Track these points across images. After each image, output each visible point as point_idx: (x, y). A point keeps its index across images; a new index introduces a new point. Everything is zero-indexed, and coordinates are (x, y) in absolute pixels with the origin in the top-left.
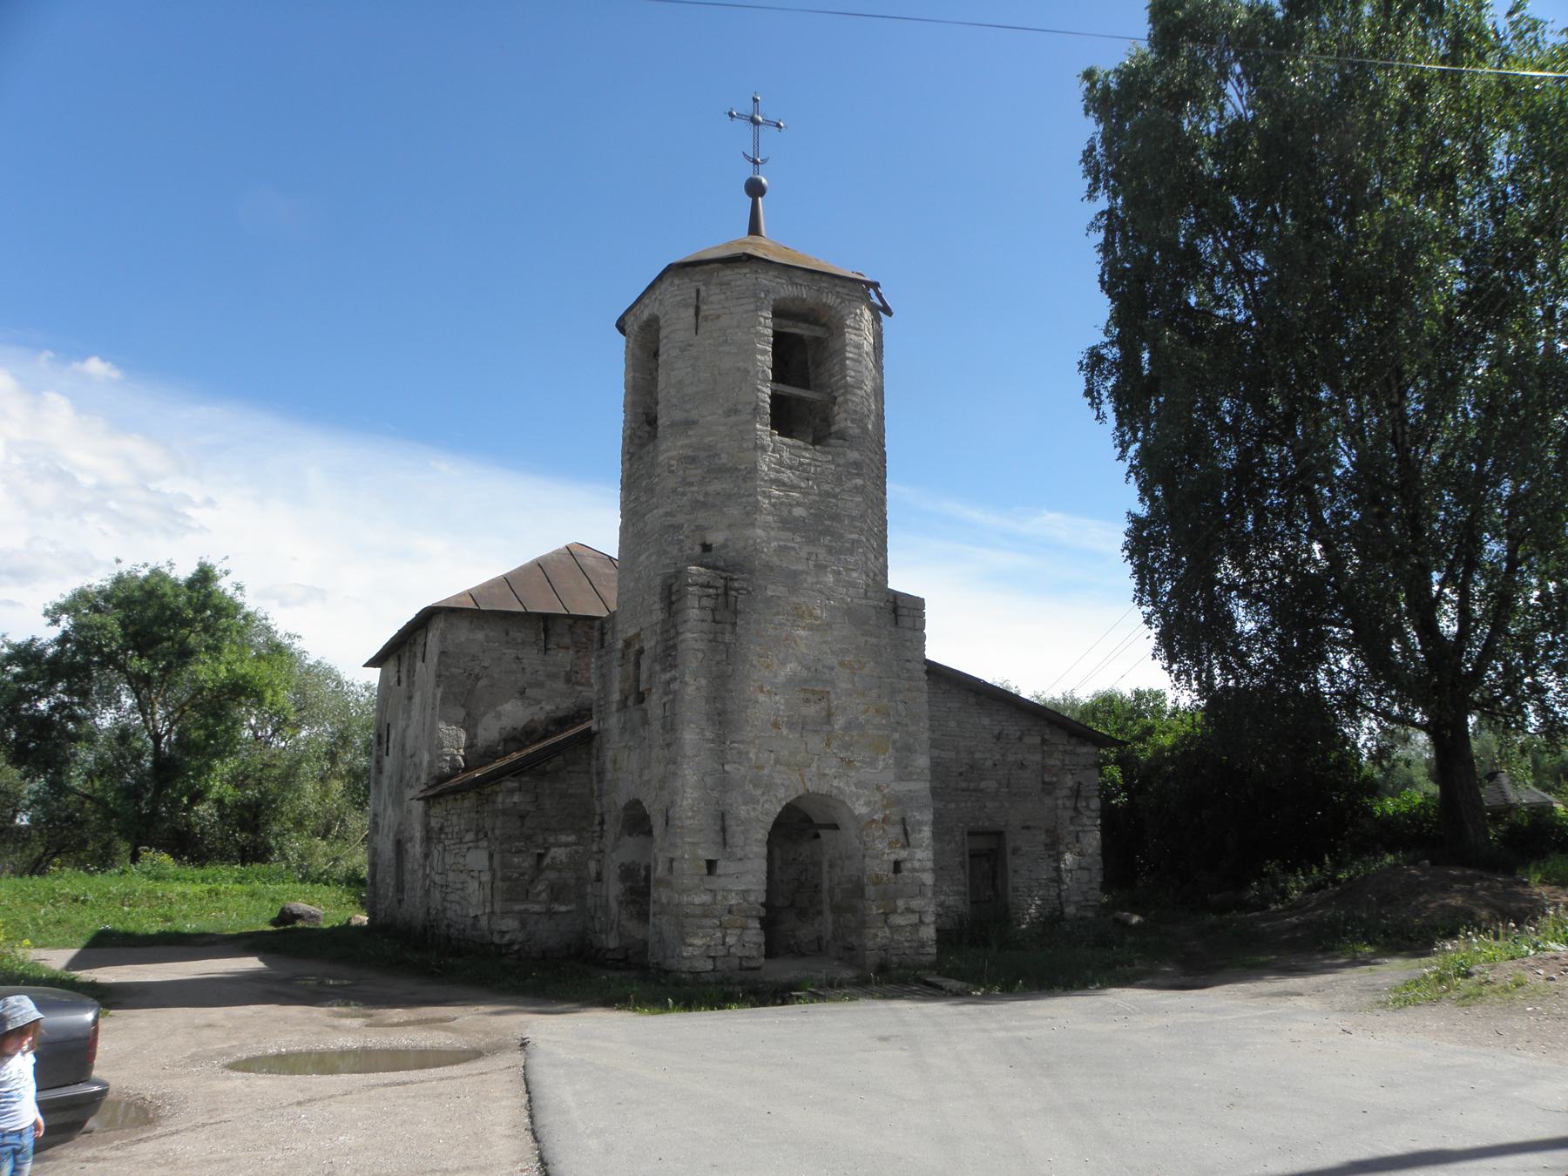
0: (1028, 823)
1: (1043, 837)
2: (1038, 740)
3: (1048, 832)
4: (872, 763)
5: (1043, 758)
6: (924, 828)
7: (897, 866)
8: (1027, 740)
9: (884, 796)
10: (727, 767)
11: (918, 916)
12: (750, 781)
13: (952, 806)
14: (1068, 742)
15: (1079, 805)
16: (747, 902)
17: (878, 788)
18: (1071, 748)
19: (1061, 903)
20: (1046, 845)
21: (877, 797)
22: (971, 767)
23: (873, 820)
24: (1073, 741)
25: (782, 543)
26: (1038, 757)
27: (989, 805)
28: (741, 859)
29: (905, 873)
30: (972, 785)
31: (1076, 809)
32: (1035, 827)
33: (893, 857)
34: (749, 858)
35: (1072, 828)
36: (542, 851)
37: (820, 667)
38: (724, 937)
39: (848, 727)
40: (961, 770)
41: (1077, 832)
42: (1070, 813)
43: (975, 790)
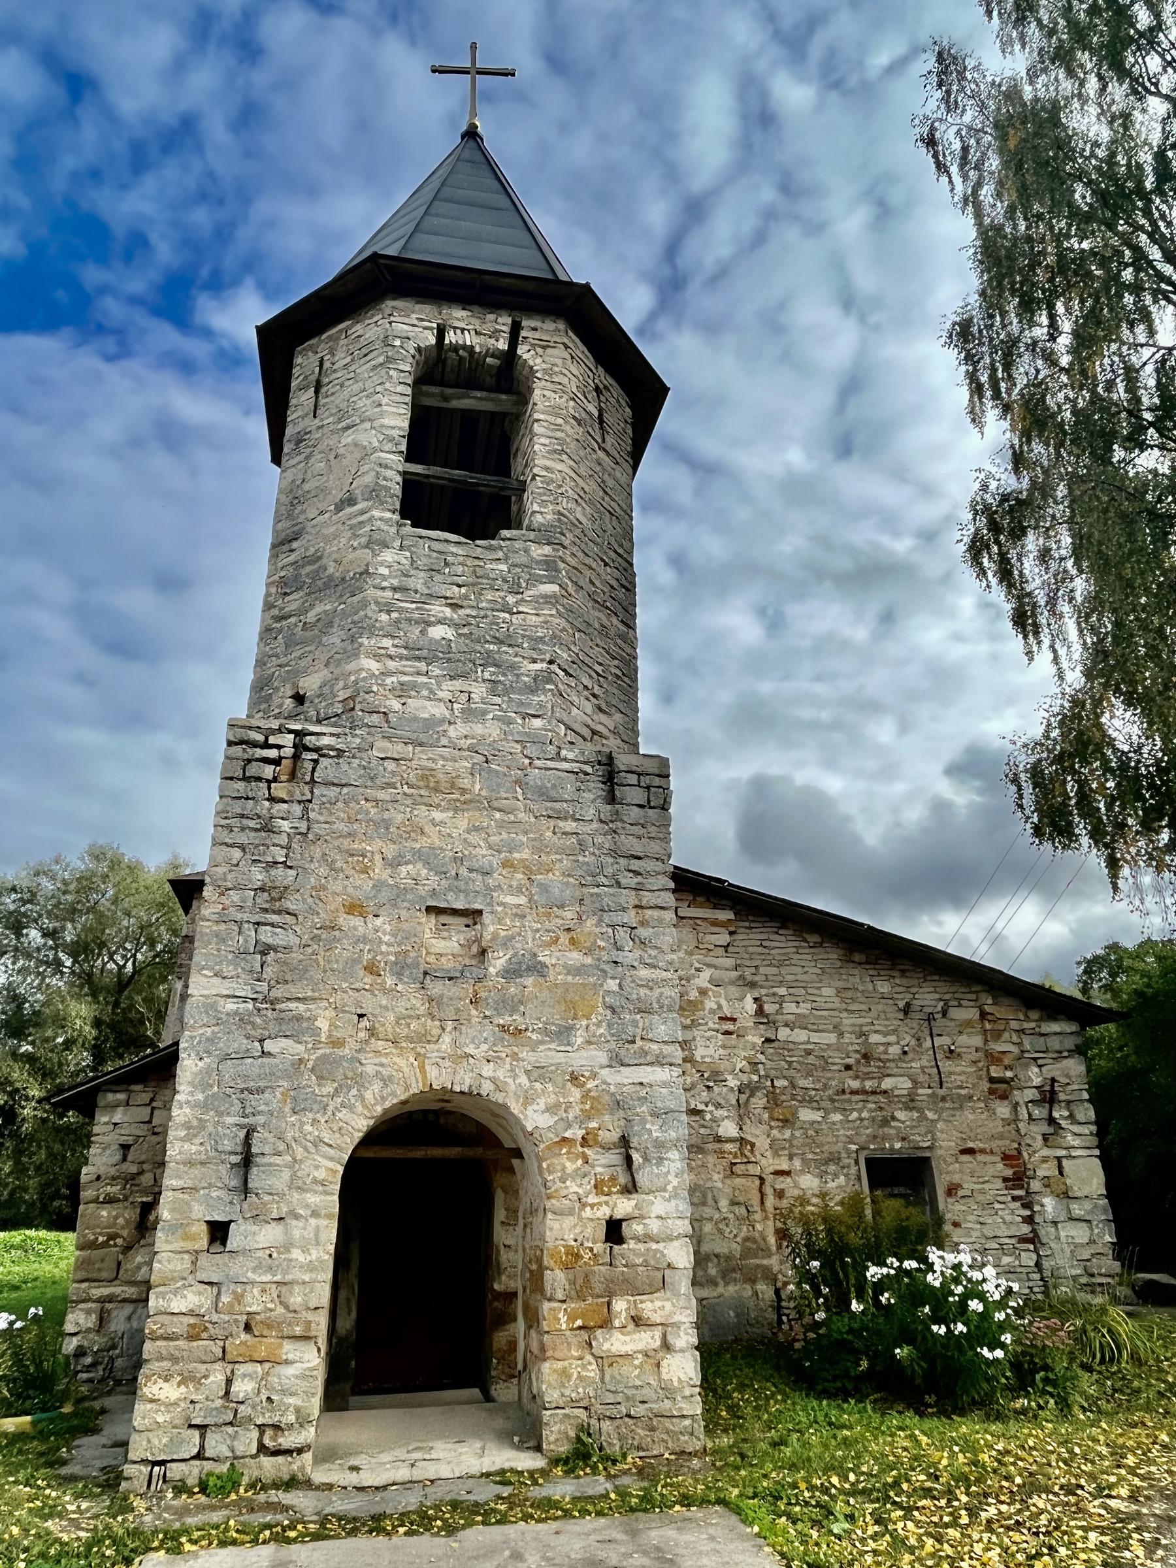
0: (971, 1145)
1: (1000, 1166)
2: (972, 1014)
3: (1006, 1157)
4: (563, 1034)
5: (986, 1041)
6: (669, 1155)
7: (614, 1231)
8: (955, 1013)
9: (586, 1096)
10: (269, 1045)
11: (658, 1333)
12: (312, 1070)
13: (837, 1117)
14: (1026, 1016)
15: (1056, 1114)
16: (287, 1307)
17: (574, 1078)
18: (1033, 1025)
19: (1042, 1279)
20: (1005, 1180)
21: (575, 1094)
22: (865, 1056)
23: (564, 1139)
24: (1034, 1015)
25: (405, 678)
26: (977, 1041)
27: (900, 1115)
29: (632, 1244)
30: (868, 1085)
31: (1051, 1121)
32: (983, 1151)
33: (604, 1212)
34: (297, 1217)
35: (1046, 1152)
36: (149, 1199)
37: (463, 872)
38: (229, 1382)
39: (512, 973)
40: (848, 1061)
41: (1059, 1159)
42: (1045, 1128)
43: (874, 1093)
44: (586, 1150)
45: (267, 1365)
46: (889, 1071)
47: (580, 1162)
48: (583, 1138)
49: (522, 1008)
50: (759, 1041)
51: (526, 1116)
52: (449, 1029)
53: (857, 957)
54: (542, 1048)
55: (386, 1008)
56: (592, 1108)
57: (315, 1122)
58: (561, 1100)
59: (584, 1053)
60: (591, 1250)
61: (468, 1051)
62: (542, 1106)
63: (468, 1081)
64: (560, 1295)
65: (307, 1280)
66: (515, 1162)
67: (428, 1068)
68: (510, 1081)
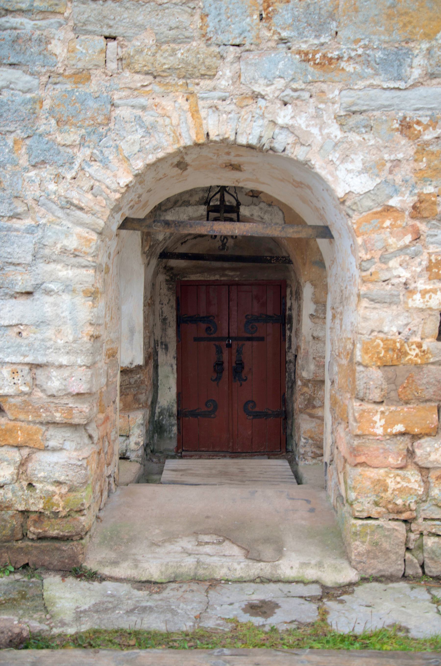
12: (51, 111)
16: (43, 391)
23: (388, 209)
28: (29, 293)
34: (48, 292)
44: (418, 223)
45: (25, 452)
47: (408, 239)
48: (414, 207)
49: (334, 25)
51: (336, 178)
52: (230, 58)
54: (361, 84)
55: (142, 27)
56: (428, 167)
57: (58, 178)
58: (386, 157)
59: (421, 91)
60: (419, 346)
61: (257, 89)
62: (358, 165)
63: (257, 132)
64: (376, 395)
65: (65, 362)
66: (322, 243)
67: (203, 113)
68: (315, 131)
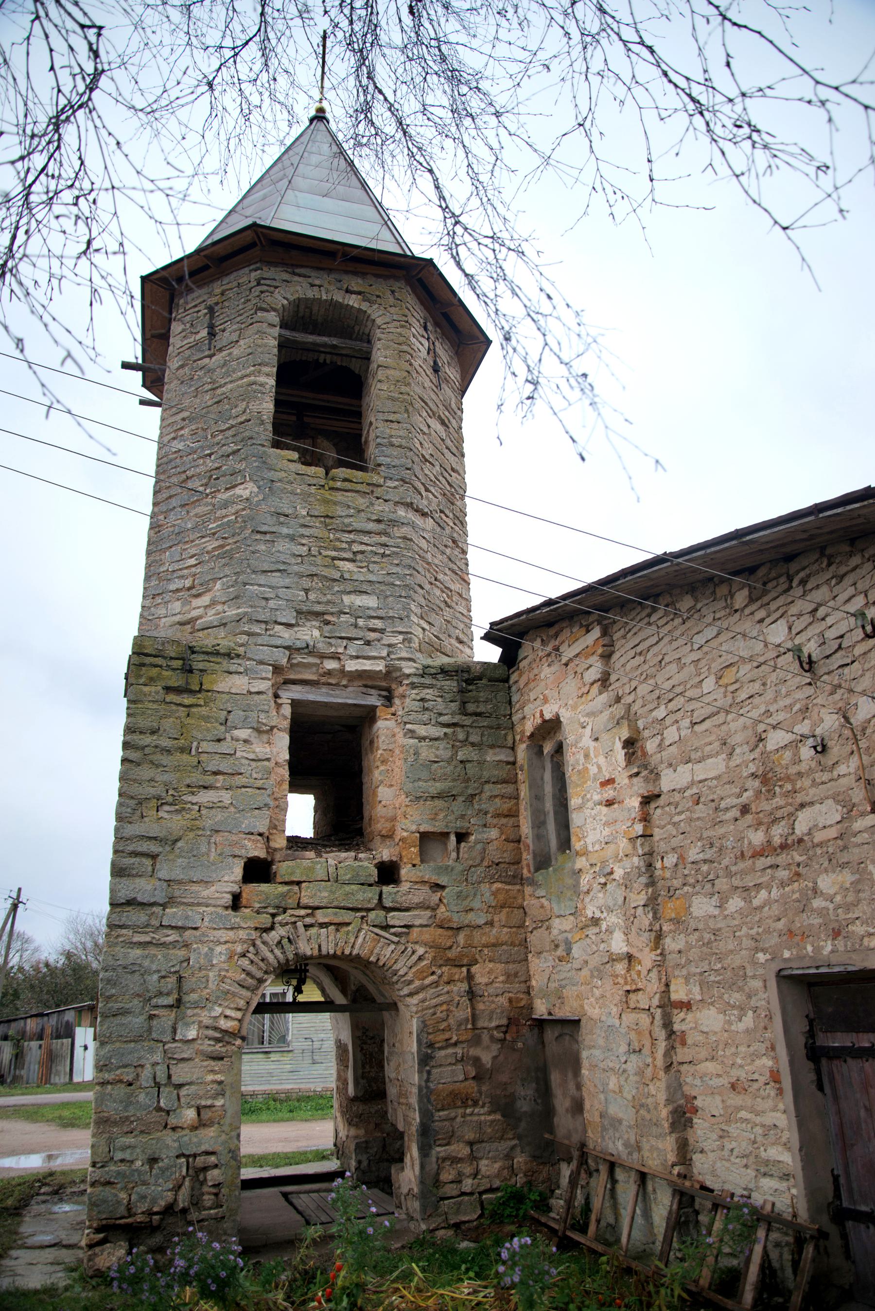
27: (827, 883)
30: (778, 833)
43: (784, 847)
46: (800, 798)
50: (636, 802)
53: (741, 598)
